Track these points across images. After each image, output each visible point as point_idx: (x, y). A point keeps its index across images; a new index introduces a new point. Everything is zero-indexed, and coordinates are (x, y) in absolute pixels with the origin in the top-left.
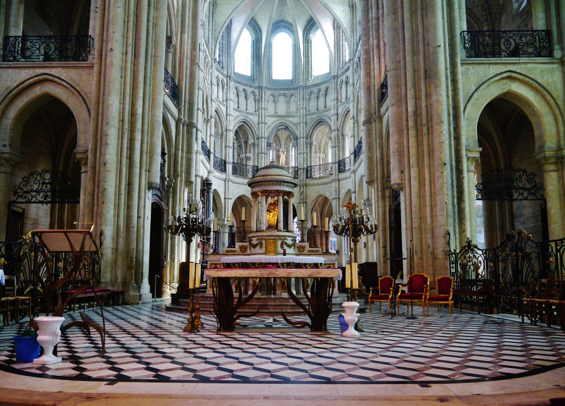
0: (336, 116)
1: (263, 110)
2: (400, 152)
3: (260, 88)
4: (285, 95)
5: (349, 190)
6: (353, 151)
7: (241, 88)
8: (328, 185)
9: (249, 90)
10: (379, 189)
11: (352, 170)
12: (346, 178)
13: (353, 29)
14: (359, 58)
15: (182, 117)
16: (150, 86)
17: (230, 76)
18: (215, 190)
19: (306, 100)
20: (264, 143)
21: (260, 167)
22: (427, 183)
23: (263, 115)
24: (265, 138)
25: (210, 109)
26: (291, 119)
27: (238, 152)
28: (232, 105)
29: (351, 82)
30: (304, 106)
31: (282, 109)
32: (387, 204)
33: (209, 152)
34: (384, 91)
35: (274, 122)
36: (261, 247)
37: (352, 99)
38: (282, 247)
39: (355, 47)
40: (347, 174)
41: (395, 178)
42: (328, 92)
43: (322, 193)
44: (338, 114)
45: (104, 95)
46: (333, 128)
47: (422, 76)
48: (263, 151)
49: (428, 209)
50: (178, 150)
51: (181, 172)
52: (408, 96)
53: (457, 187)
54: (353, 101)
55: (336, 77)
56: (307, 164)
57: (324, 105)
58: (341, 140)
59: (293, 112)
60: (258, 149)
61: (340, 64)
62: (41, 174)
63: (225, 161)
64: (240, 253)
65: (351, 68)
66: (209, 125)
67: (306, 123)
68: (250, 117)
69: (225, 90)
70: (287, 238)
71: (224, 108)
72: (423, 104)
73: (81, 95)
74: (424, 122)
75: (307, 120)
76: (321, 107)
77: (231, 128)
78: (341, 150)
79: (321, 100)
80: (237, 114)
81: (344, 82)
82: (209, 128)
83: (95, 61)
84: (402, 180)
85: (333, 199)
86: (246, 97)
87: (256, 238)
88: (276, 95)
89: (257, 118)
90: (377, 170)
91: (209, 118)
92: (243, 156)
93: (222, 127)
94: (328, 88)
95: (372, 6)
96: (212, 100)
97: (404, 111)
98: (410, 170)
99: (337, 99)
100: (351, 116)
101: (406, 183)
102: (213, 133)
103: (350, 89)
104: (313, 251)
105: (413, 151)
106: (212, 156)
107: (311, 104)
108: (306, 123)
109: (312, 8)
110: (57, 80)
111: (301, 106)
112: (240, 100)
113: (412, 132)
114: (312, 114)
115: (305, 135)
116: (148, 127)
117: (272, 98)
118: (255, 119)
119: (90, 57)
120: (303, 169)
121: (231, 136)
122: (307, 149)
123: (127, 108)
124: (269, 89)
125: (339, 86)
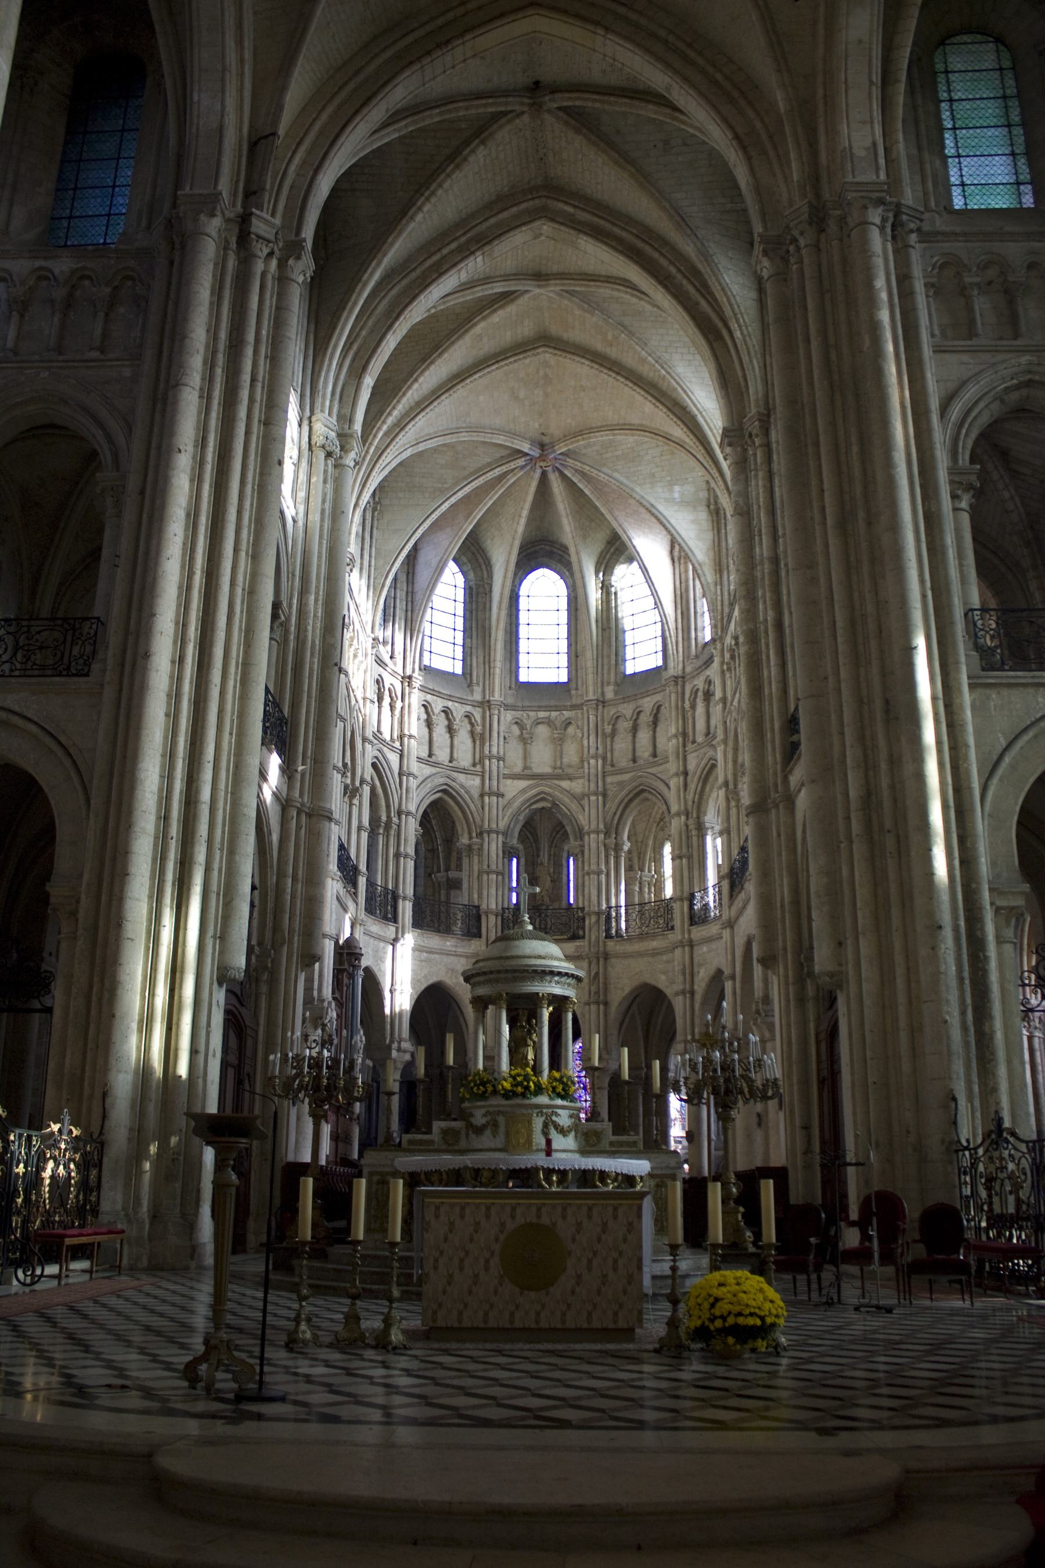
0: (682, 778)
1: (494, 761)
2: (834, 893)
3: (485, 704)
4: (549, 722)
5: (719, 972)
6: (725, 870)
7: (438, 704)
8: (665, 958)
9: (459, 711)
10: (791, 980)
11: (725, 917)
12: (710, 940)
13: (719, 568)
14: (736, 638)
15: (296, 794)
16: (231, 734)
17: (410, 677)
18: (368, 970)
19: (604, 734)
20: (494, 846)
21: (484, 906)
22: (900, 971)
23: (495, 773)
24: (498, 833)
25: (359, 761)
26: (565, 784)
27: (426, 867)
28: (416, 748)
29: (718, 694)
30: (600, 751)
31: (542, 758)
32: (811, 1016)
33: (356, 869)
34: (795, 738)
35: (524, 791)
36: (495, 1134)
37: (720, 735)
38: (545, 1133)
39: (726, 610)
40: (714, 929)
41: (822, 958)
44: (686, 773)
45: (125, 757)
46: (674, 808)
47: (879, 716)
48: (493, 867)
49: (903, 1036)
50: (285, 876)
51: (291, 931)
52: (849, 760)
53: (972, 981)
54: (725, 741)
55: (680, 680)
56: (608, 900)
57: (651, 749)
58: (695, 839)
59: (570, 766)
60: (480, 862)
61: (689, 647)
63: (393, 892)
64: (444, 1147)
65: (717, 660)
66: (356, 801)
67: (605, 795)
68: (461, 778)
69: (397, 712)
70: (559, 1111)
71: (393, 758)
72: (885, 782)
73: (70, 755)
74: (888, 824)
75: (608, 787)
76: (644, 751)
77: (412, 808)
78: (696, 866)
79: (644, 736)
80: (428, 770)
81: (700, 694)
82: (355, 810)
84: (840, 965)
85: (677, 994)
86: (450, 730)
87: (483, 1111)
88: (528, 723)
89: (477, 781)
90: (784, 929)
91: (357, 784)
92: (441, 876)
93: (388, 806)
94: (659, 707)
95: (760, 531)
96: (364, 740)
97: (839, 797)
98: (857, 939)
99: (685, 735)
100: (721, 780)
101: (851, 973)
102: (366, 822)
103: (717, 710)
104: (621, 1144)
105: (862, 893)
106: (362, 881)
107: (617, 746)
108: (605, 795)
109: (617, 513)
110: (15, 720)
111: (592, 751)
112: (435, 735)
113: (859, 850)
114: (622, 771)
115: (602, 826)
116: (223, 832)
117: (516, 730)
118: (473, 783)
119: (96, 667)
120: (598, 914)
121: (411, 828)
122: (607, 862)
123: (178, 786)
124: (508, 707)
125: (687, 704)
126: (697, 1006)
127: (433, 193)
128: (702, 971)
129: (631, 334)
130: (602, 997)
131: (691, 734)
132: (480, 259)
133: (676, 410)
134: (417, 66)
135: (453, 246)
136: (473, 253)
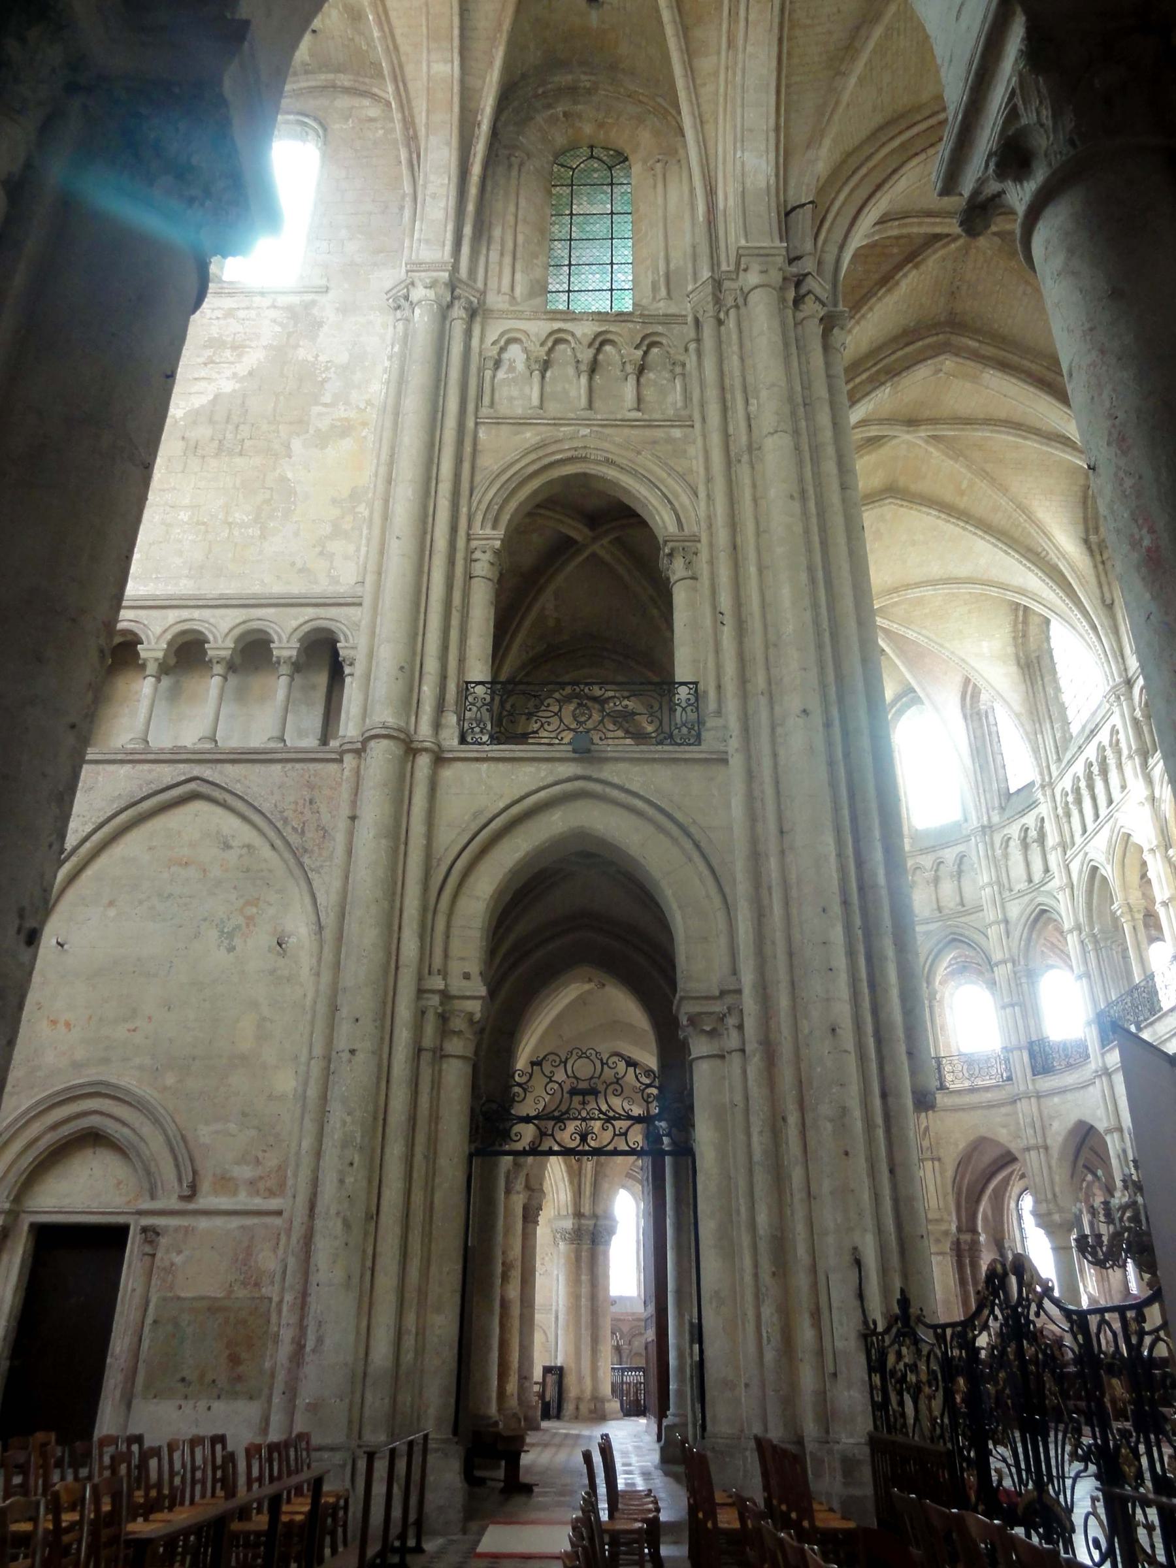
0: (1002, 926)
8: (1003, 1110)
42: (964, 868)
43: (983, 1131)
44: (1006, 922)
46: (997, 956)
57: (958, 899)
58: (1025, 986)
62: (565, 1063)
73: (689, 835)
79: (947, 887)
83: (734, 744)
85: (1028, 1149)
110: (615, 793)
125: (999, 852)
126: (1054, 1163)
127: (863, 316)
128: (1056, 1125)
129: (992, 480)
130: (935, 1153)
131: (1005, 881)
132: (888, 390)
133: (1029, 555)
134: (923, 156)
135: (864, 376)
136: (883, 384)
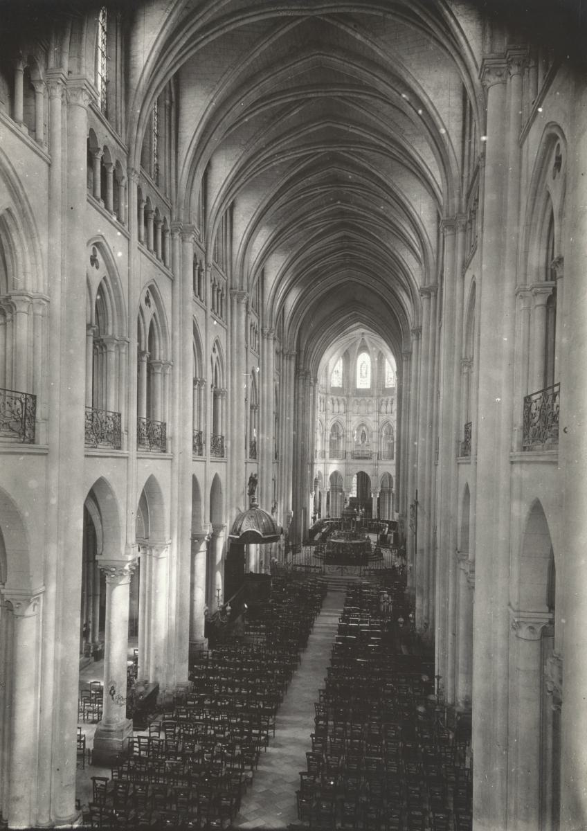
7: (335, 398)
79: (389, 405)
